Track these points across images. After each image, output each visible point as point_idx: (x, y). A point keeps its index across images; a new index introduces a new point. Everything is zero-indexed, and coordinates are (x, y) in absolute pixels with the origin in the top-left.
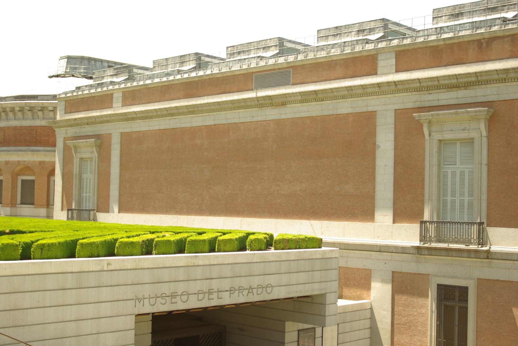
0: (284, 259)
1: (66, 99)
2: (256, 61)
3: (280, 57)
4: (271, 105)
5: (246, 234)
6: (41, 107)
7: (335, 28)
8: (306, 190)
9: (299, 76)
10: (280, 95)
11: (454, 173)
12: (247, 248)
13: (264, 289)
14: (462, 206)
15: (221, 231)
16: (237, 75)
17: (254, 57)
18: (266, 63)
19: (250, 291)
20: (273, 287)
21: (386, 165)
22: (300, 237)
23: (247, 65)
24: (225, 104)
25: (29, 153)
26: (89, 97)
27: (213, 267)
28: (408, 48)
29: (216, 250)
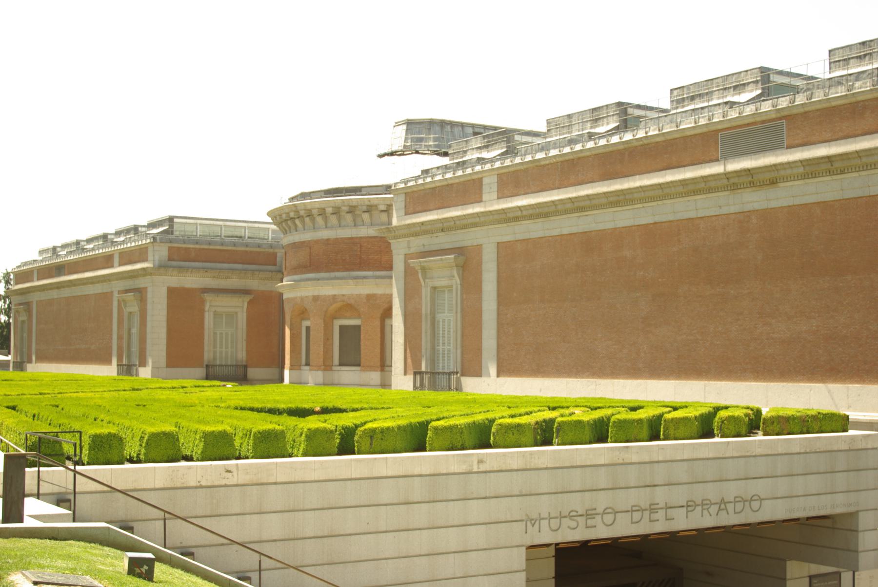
0: (780, 451)
1: (405, 191)
2: (721, 111)
3: (764, 100)
4: (752, 185)
5: (714, 408)
6: (368, 205)
8: (817, 331)
9: (798, 131)
10: (766, 167)
12: (715, 432)
13: (747, 504)
15: (670, 404)
16: (690, 136)
17: (719, 104)
18: (740, 113)
19: (723, 506)
20: (763, 499)
22: (810, 413)
23: (707, 117)
24: (670, 187)
25: (351, 281)
26: (442, 186)
27: (656, 465)
29: (662, 437)
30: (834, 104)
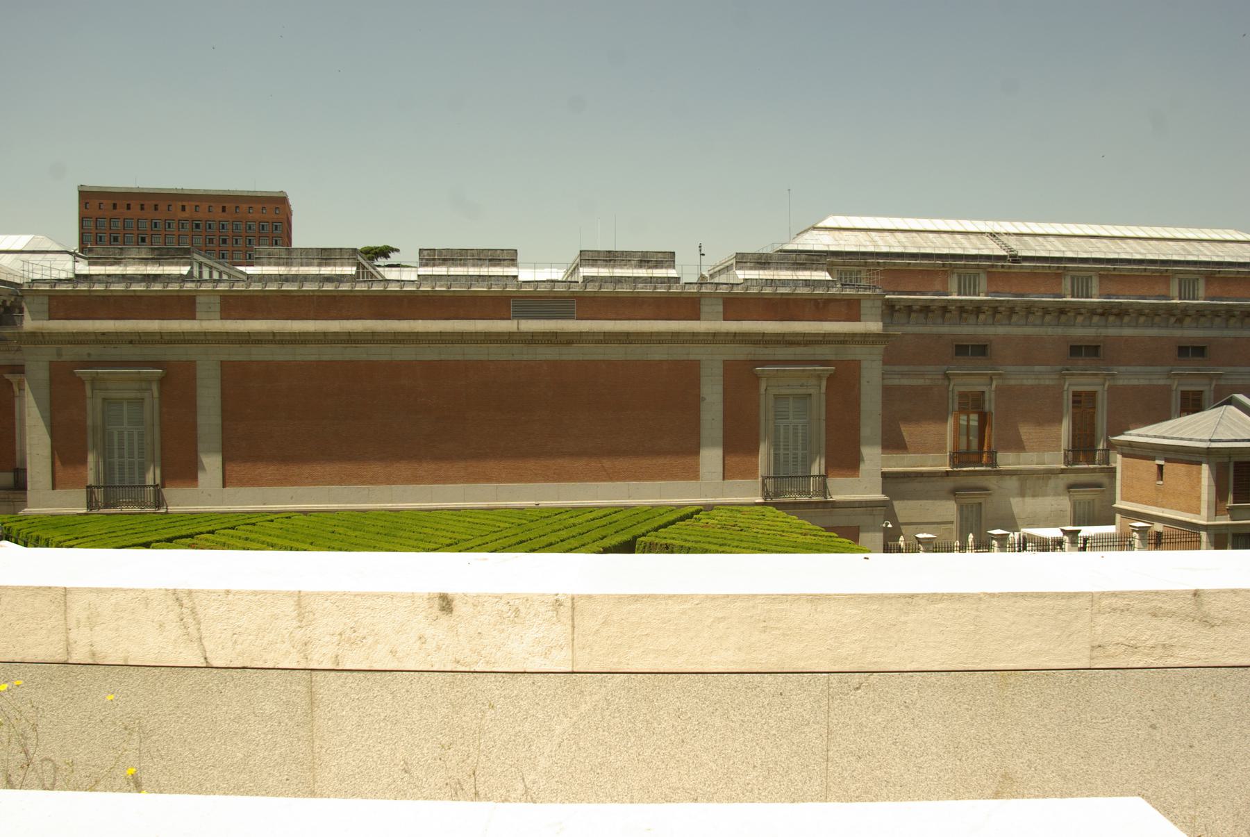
7: (607, 251)
11: (786, 428)
14: (795, 458)
21: (713, 419)
28: (739, 296)
30: (620, 295)
